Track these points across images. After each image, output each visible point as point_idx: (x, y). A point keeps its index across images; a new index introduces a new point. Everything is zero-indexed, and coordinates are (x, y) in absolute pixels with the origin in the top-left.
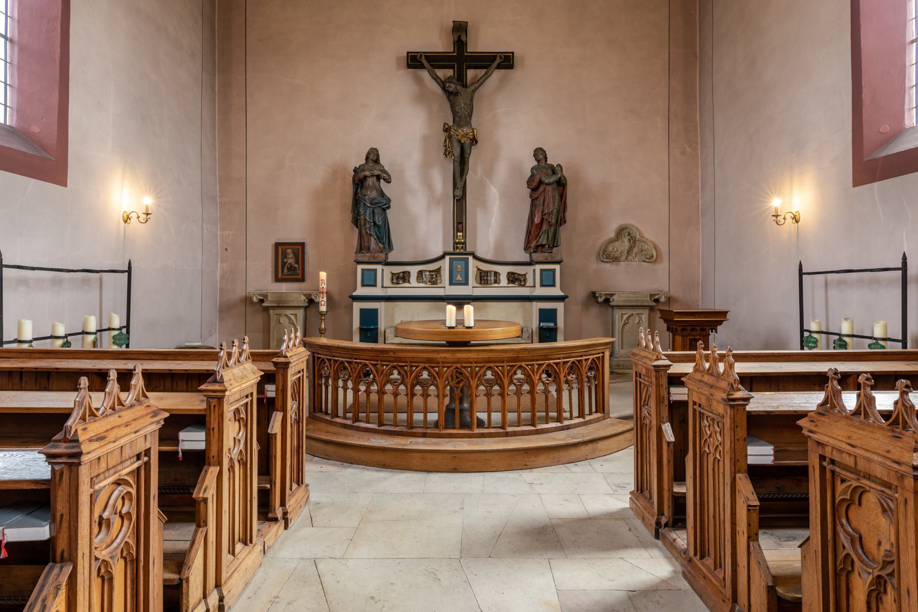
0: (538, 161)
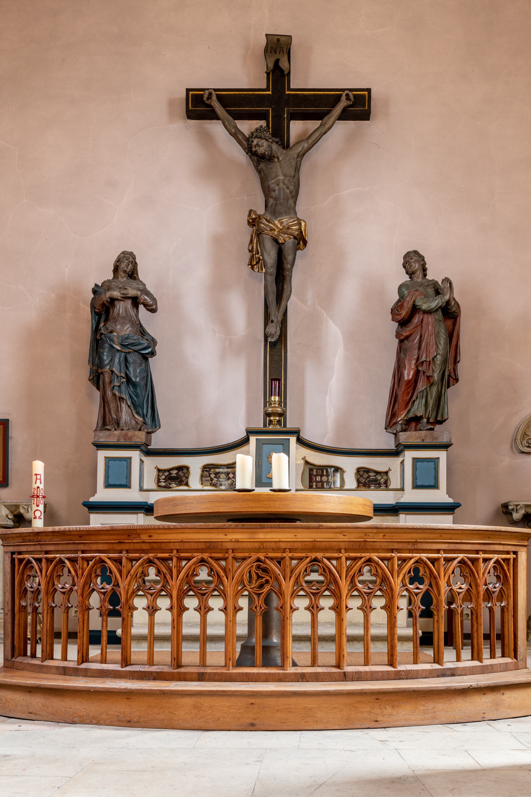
0: (411, 274)
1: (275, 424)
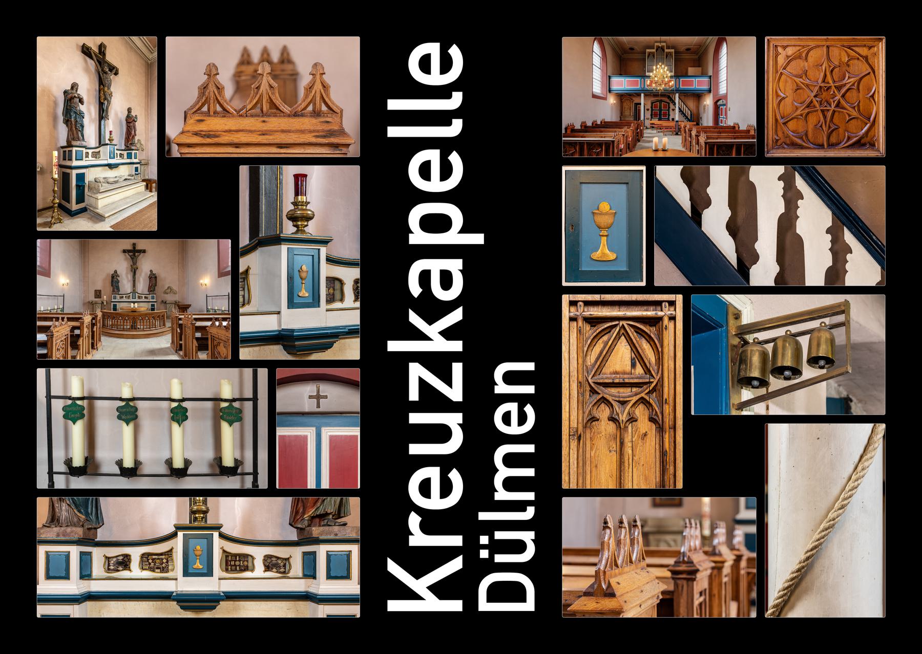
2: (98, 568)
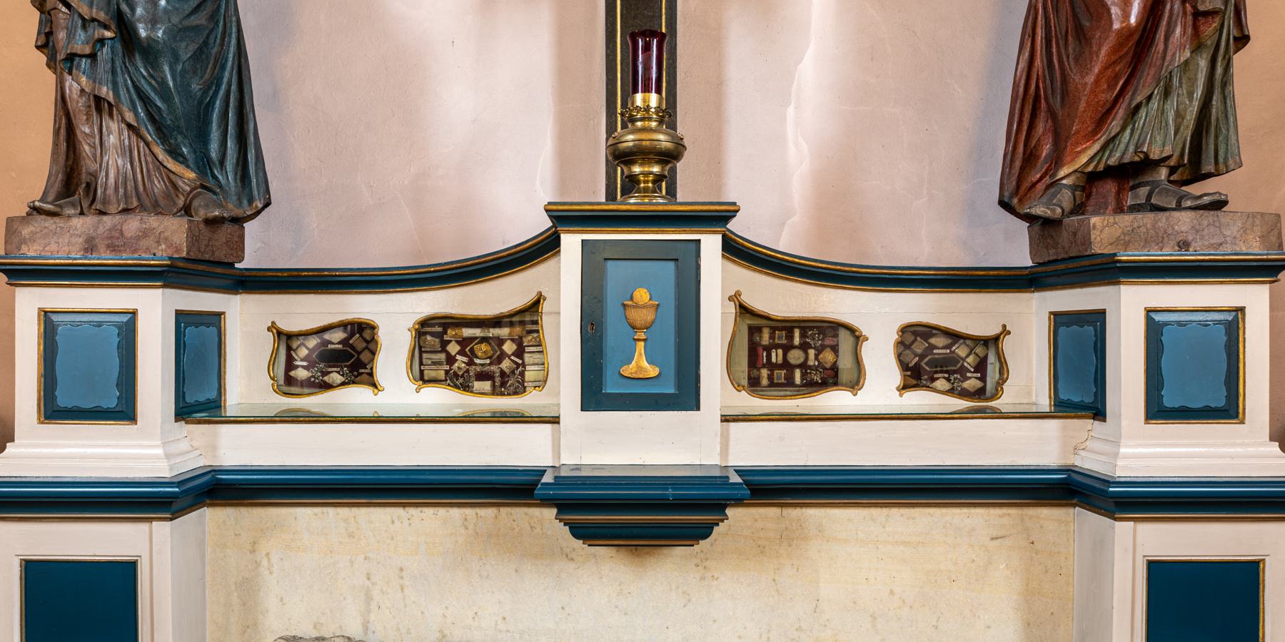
1: (646, 190)
2: (246, 376)
